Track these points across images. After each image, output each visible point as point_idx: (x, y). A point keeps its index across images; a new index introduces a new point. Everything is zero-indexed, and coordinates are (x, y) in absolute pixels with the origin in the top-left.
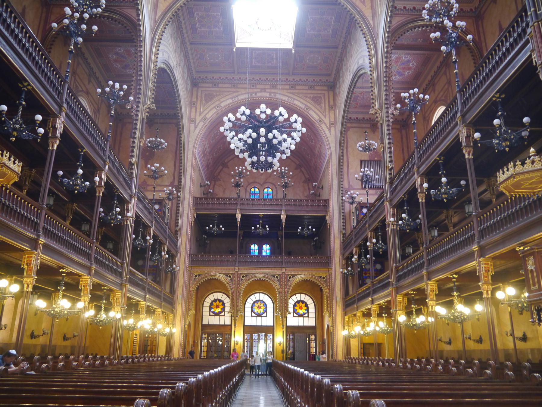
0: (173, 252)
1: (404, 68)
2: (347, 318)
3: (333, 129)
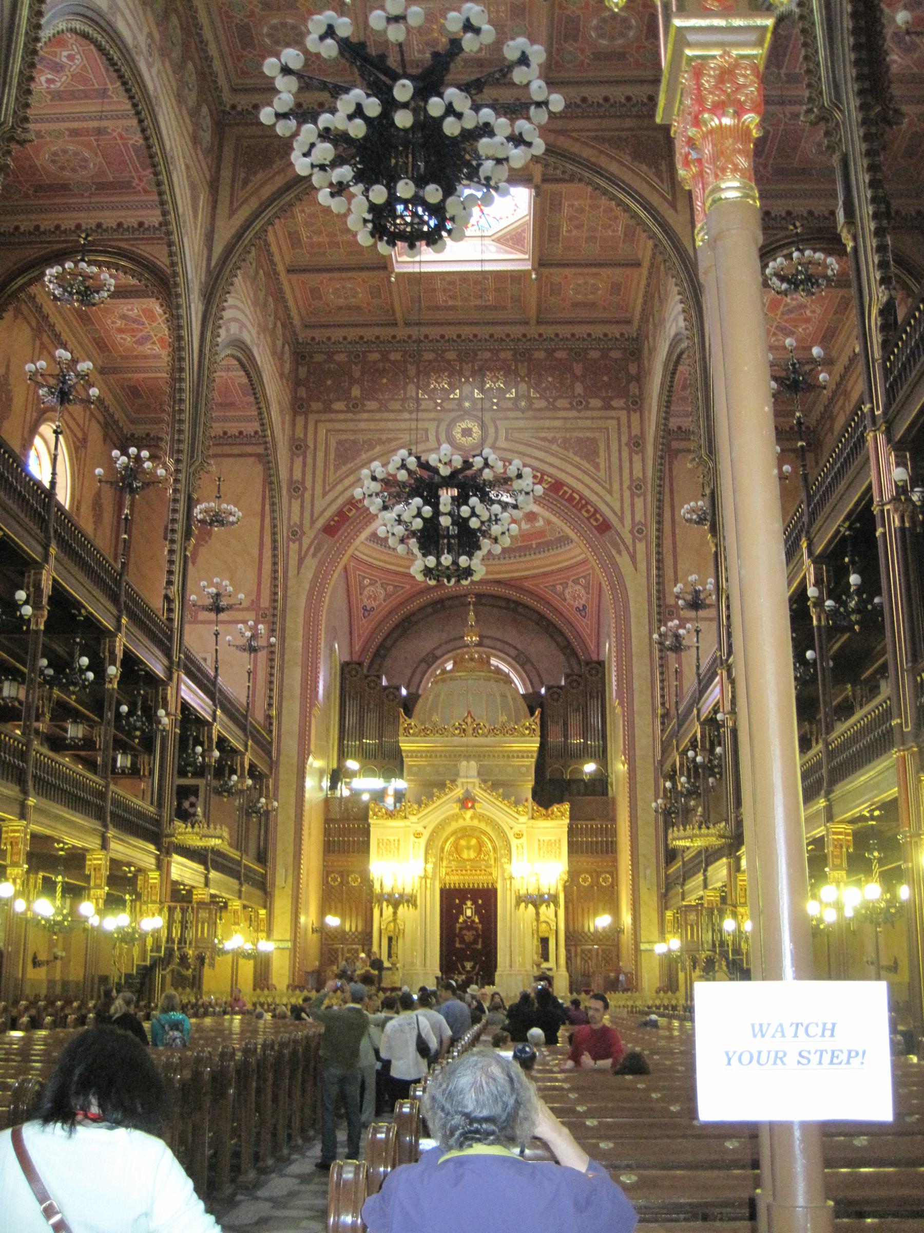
0: (262, 767)
2: (669, 914)
3: (637, 458)
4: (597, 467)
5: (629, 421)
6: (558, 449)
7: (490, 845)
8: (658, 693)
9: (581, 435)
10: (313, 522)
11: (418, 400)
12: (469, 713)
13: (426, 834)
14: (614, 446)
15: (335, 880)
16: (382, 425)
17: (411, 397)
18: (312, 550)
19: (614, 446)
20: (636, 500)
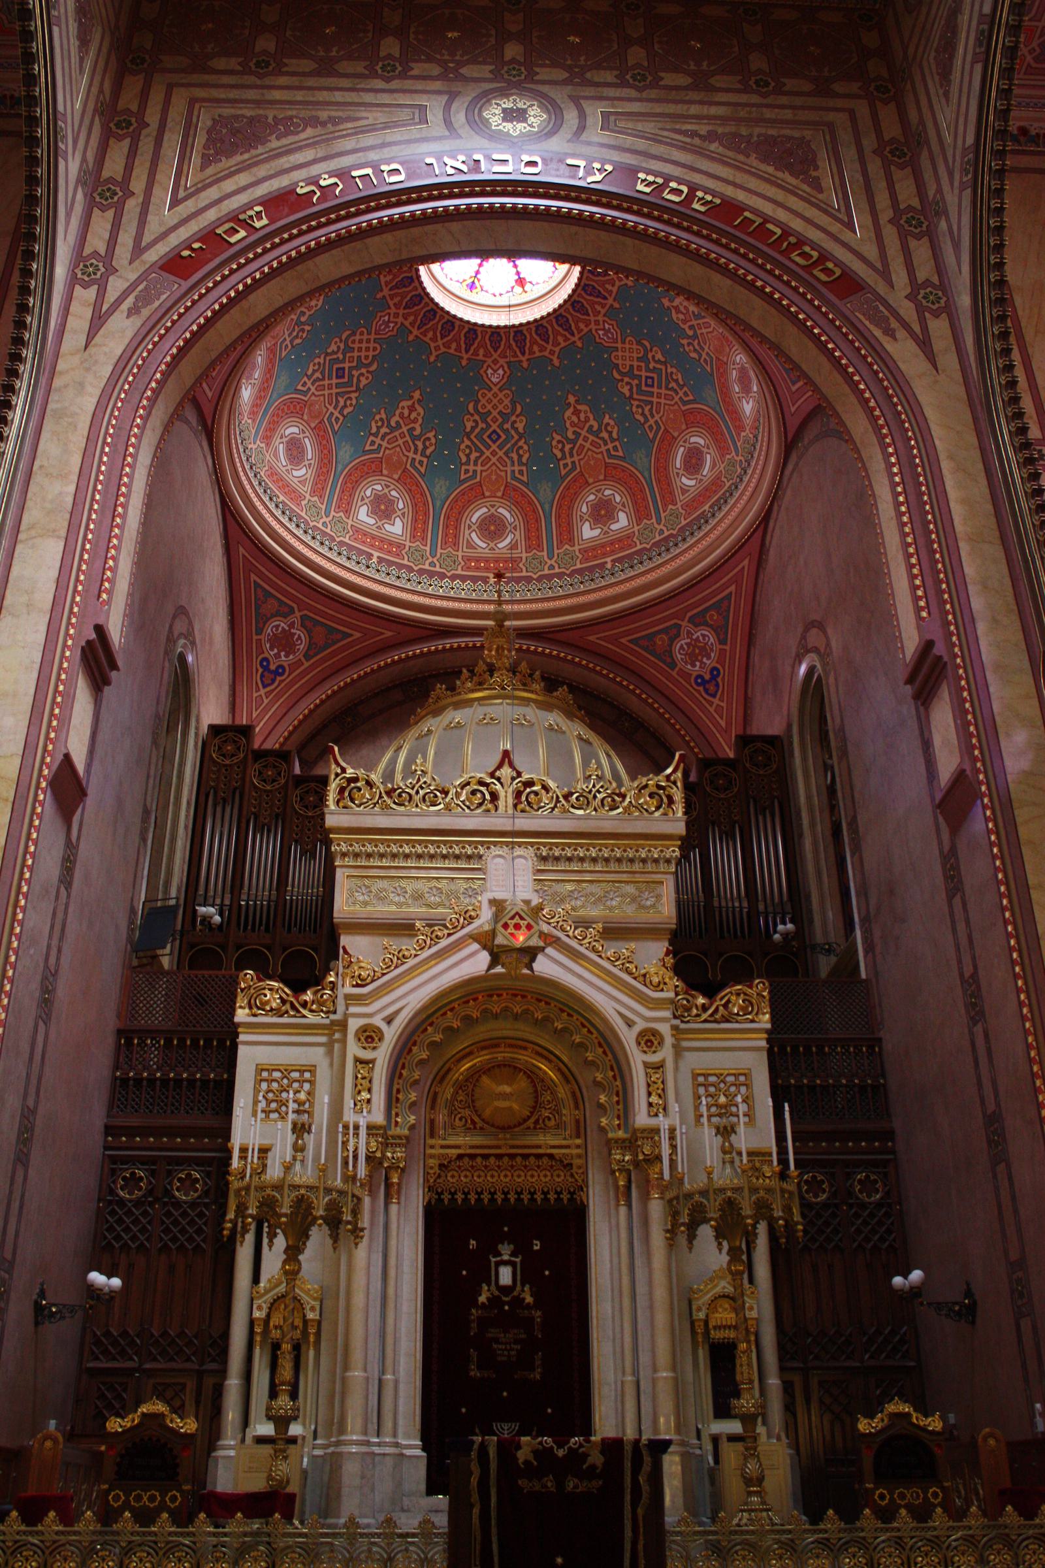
4: (817, 185)
5: (874, 115)
6: (721, 150)
7: (562, 1092)
9: (772, 132)
10: (138, 250)
12: (506, 754)
16: (323, 96)
18: (130, 300)
19: (849, 154)
20: (913, 243)
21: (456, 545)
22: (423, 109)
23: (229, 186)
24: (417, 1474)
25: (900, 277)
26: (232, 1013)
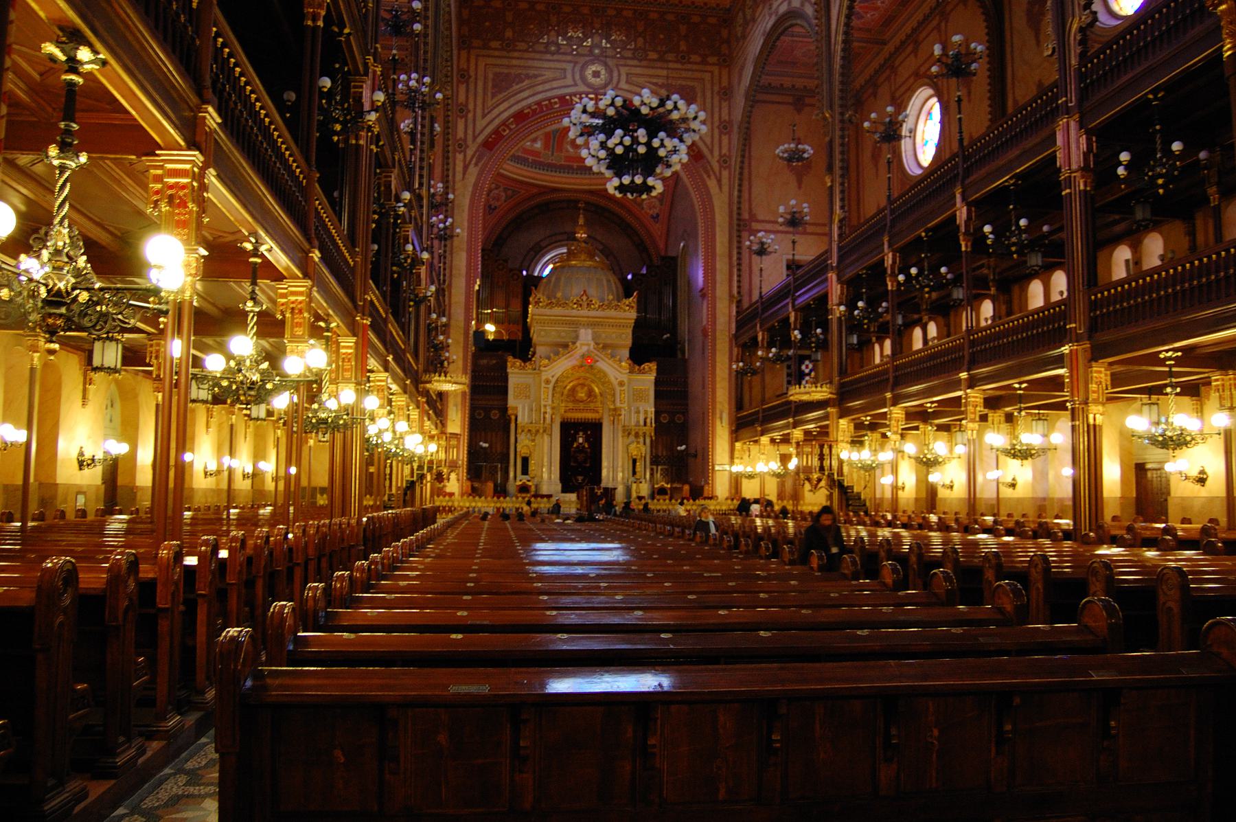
1: (867, 7)
2: (738, 445)
8: (735, 284)
9: (684, 83)
10: (475, 138)
11: (558, 45)
12: (585, 291)
13: (554, 380)
14: (708, 94)
15: (480, 414)
16: (530, 63)
17: (553, 42)
18: (474, 160)
19: (708, 94)
20: (723, 137)
21: (561, 151)
22: (565, 70)
23: (502, 108)
24: (559, 487)
25: (716, 153)
26: (506, 368)
